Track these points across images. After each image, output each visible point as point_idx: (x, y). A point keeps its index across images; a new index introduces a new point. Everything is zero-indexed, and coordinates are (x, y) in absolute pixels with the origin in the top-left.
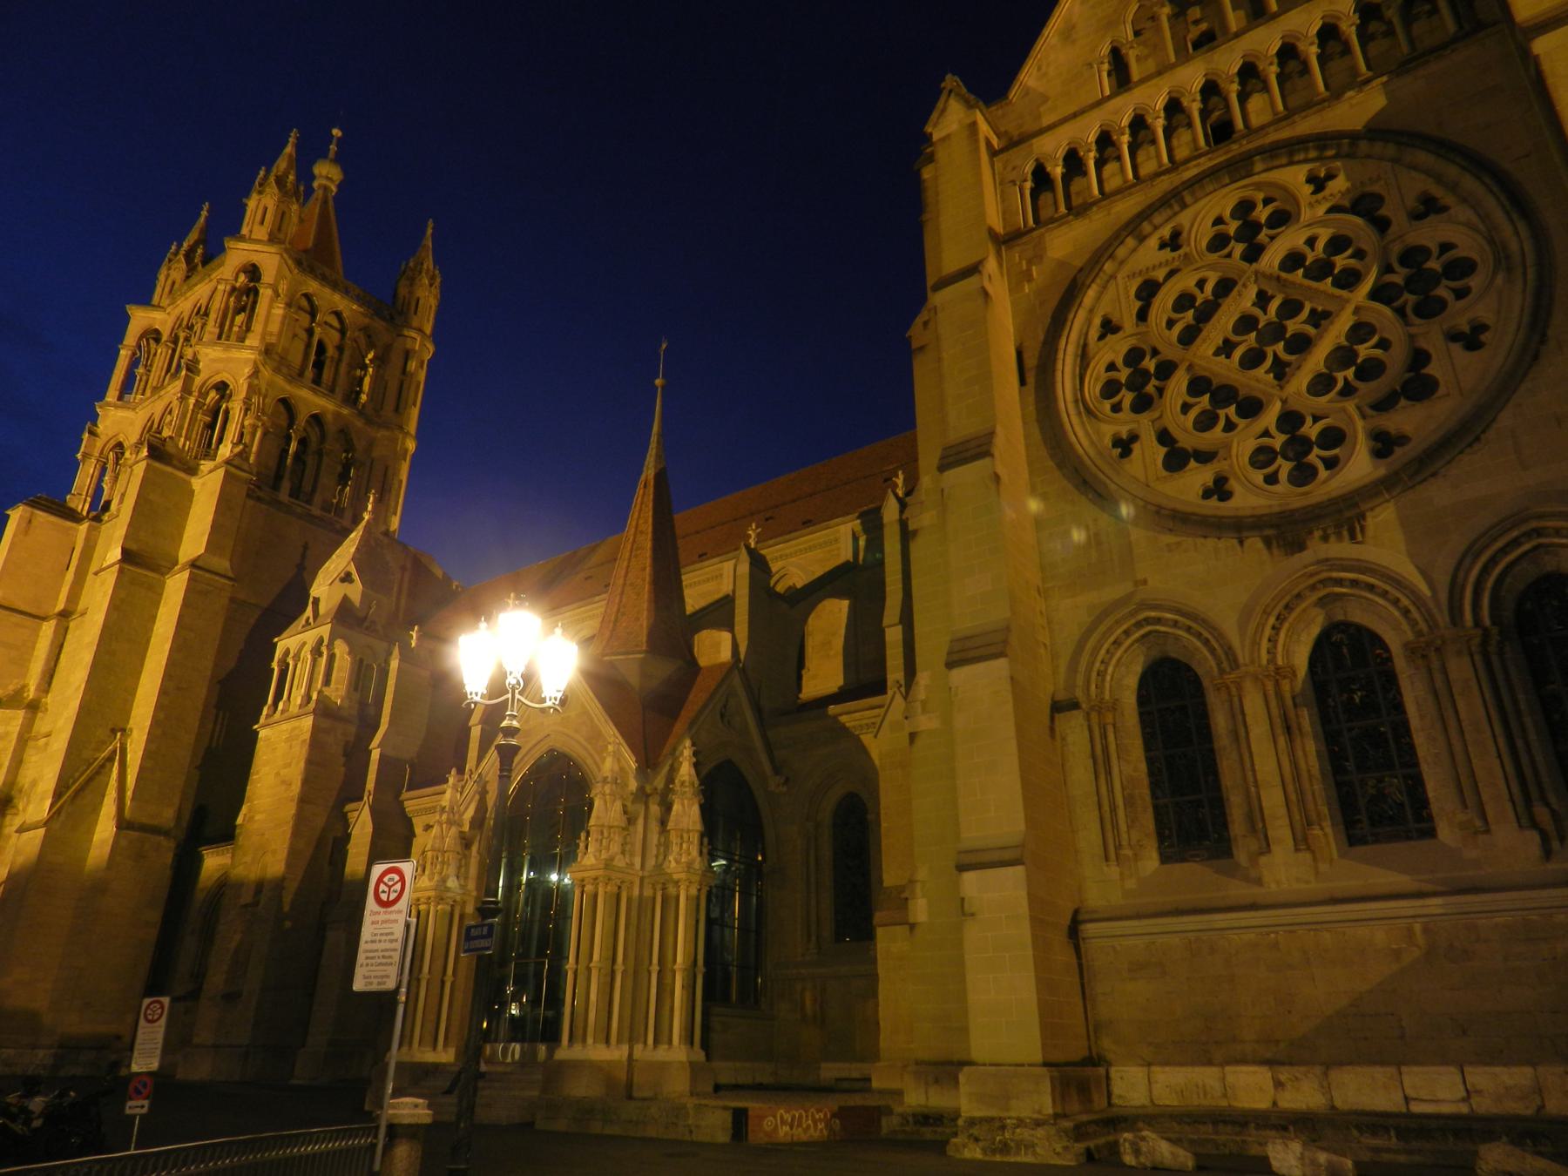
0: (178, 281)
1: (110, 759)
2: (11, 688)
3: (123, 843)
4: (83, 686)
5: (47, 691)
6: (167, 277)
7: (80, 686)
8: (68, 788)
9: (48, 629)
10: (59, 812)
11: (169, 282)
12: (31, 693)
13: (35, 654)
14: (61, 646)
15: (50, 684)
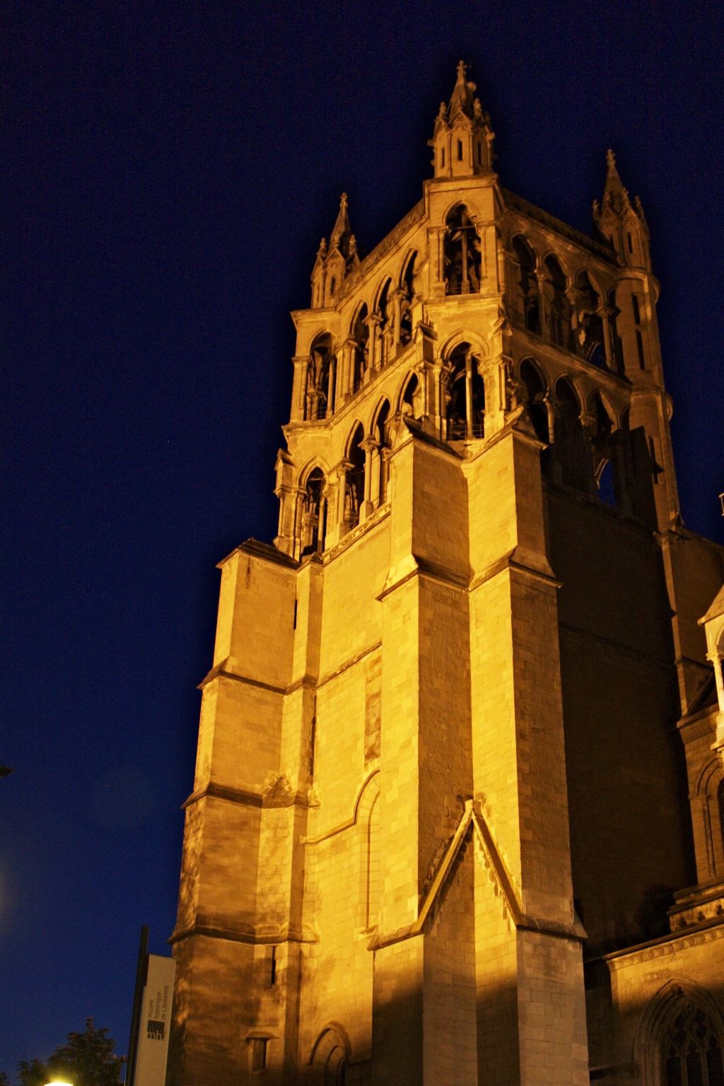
0: (339, 277)
1: (468, 837)
2: (267, 781)
3: (528, 948)
4: (415, 740)
5: (310, 781)
6: (325, 275)
7: (409, 742)
8: (432, 879)
9: (294, 703)
10: (431, 915)
11: (329, 281)
12: (293, 783)
13: (284, 735)
14: (314, 721)
15: (312, 773)
